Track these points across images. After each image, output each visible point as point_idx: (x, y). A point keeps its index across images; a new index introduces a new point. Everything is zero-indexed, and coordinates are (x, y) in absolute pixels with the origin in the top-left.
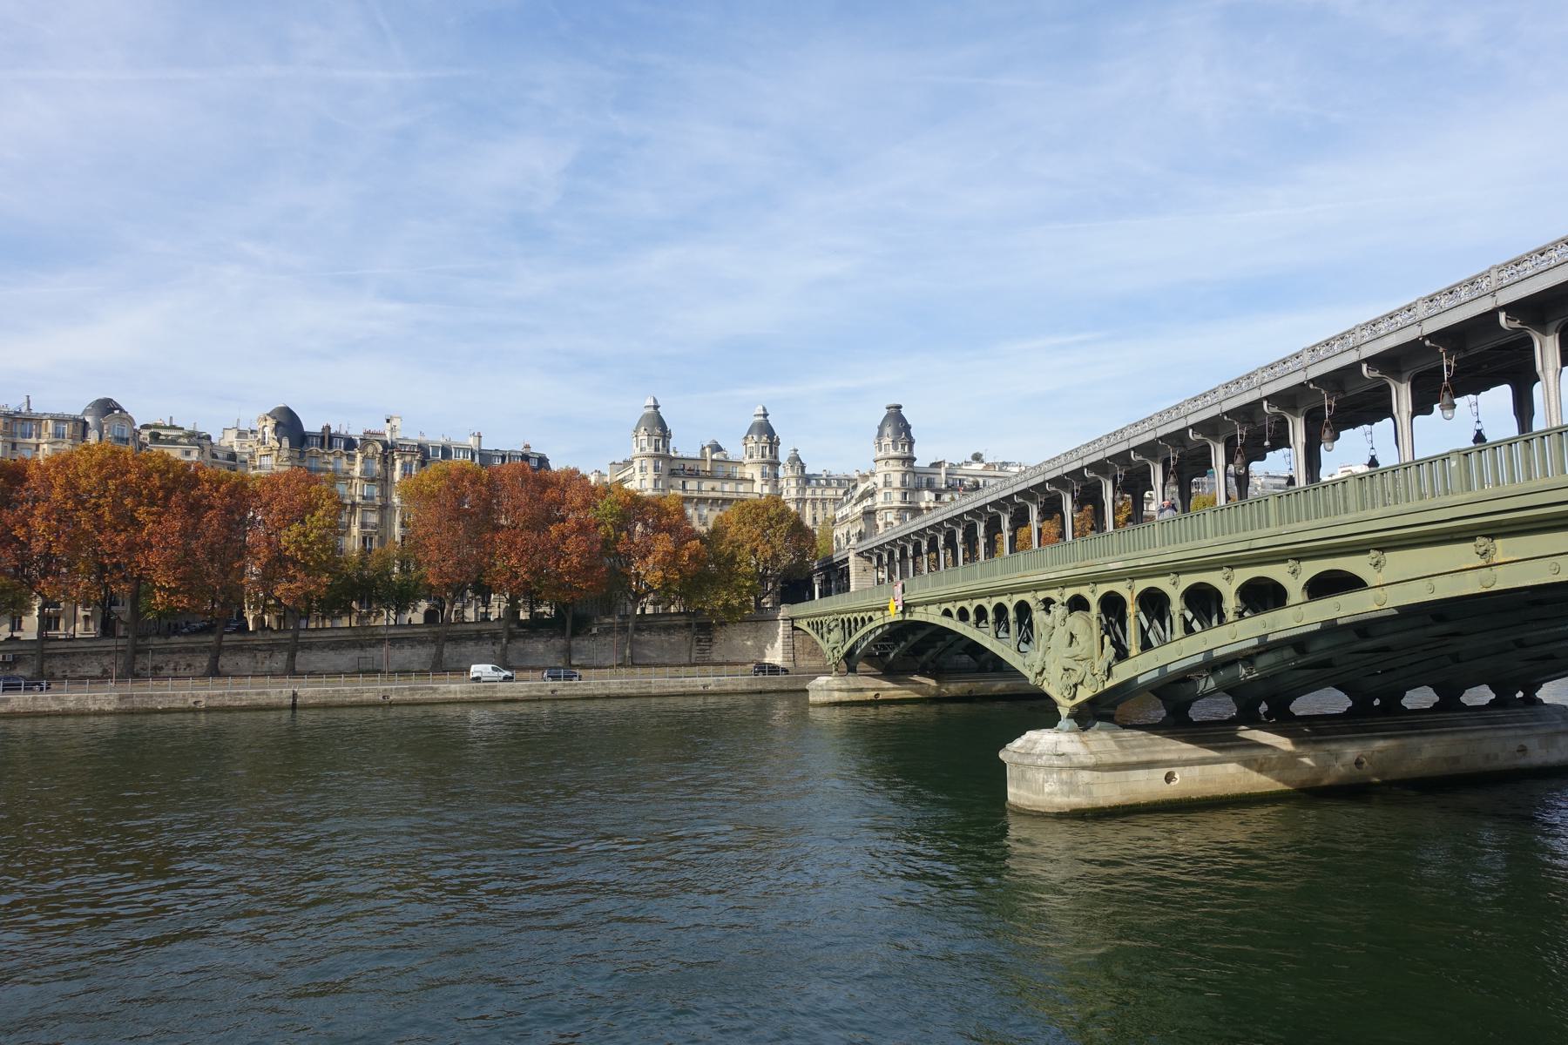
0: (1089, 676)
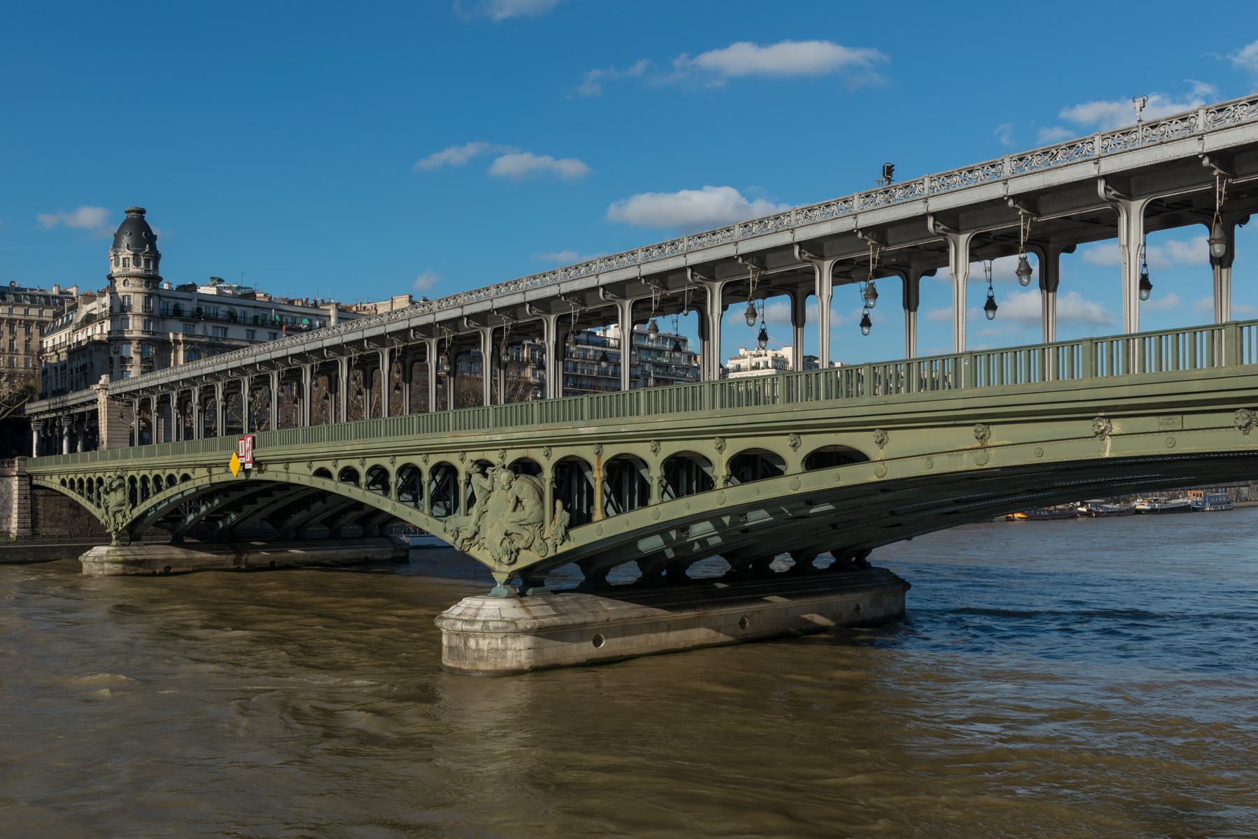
0: (538, 542)
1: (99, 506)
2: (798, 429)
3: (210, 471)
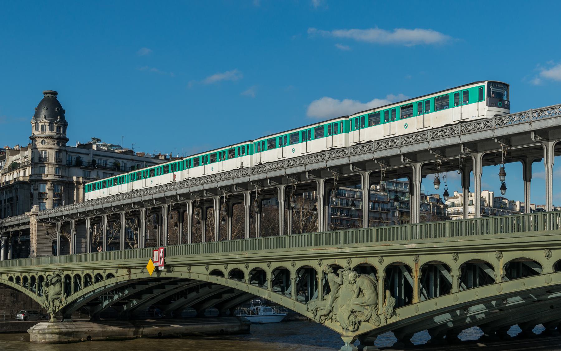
0: (374, 317)
1: (40, 295)
3: (129, 272)
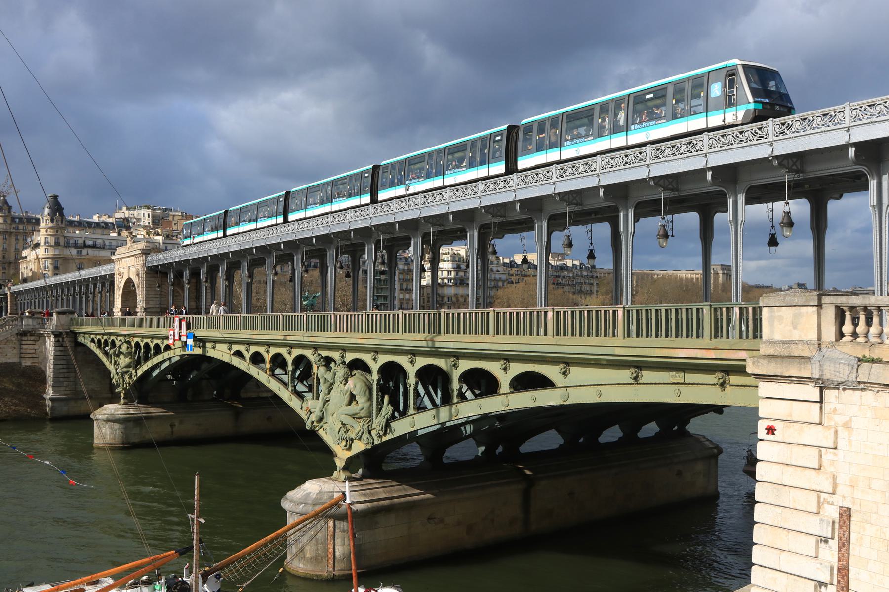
2: (507, 358)
